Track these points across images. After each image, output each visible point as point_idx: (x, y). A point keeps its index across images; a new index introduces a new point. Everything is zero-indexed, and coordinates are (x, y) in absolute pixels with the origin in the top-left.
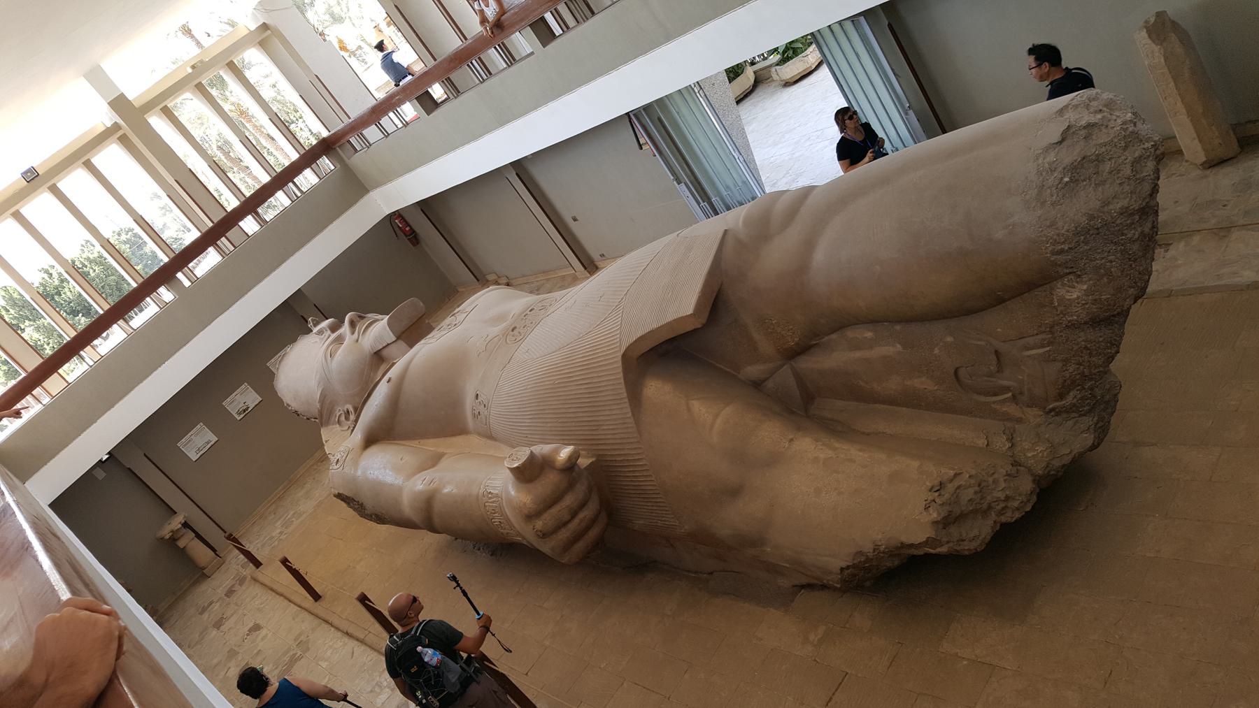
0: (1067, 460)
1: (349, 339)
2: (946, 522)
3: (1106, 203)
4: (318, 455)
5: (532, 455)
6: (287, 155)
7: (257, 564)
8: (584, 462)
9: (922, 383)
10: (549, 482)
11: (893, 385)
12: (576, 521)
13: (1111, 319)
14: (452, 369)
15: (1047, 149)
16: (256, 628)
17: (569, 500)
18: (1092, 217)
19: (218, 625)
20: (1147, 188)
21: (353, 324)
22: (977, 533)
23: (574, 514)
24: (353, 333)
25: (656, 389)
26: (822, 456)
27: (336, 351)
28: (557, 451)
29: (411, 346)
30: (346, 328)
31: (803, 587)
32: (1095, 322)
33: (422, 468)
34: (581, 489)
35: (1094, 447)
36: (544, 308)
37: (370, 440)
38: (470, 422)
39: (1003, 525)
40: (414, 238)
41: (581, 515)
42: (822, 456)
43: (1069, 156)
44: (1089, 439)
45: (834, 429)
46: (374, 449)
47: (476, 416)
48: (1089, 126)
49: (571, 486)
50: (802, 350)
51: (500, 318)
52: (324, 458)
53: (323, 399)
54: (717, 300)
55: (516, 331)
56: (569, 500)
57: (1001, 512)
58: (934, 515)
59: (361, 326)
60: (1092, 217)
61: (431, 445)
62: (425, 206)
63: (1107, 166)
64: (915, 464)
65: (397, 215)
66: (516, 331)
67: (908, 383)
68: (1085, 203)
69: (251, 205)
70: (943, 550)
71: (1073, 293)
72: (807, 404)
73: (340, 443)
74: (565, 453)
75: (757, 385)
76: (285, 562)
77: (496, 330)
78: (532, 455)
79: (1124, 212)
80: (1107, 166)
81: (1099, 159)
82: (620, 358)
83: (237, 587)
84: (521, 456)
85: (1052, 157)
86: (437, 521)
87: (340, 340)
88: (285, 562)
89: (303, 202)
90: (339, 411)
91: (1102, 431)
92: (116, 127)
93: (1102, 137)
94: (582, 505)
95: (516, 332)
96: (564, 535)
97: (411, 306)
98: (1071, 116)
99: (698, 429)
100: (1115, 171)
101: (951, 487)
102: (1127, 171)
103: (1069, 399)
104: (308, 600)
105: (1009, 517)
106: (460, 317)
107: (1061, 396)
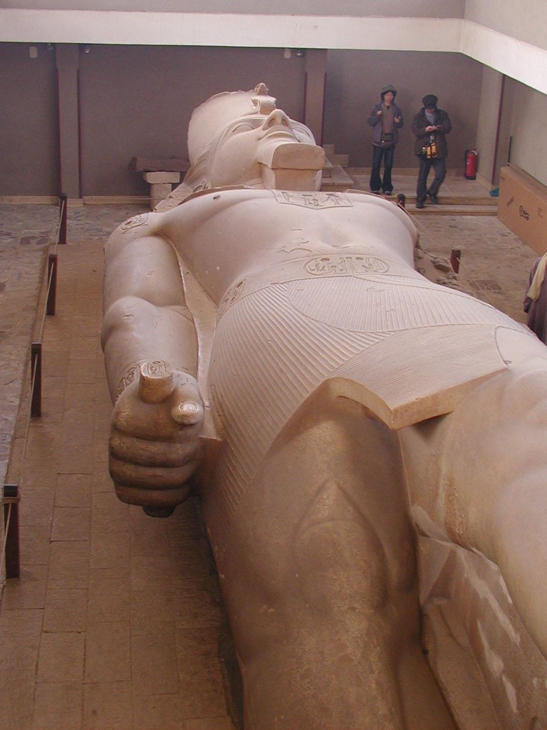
1: (259, 131)
5: (169, 380)
8: (210, 432)
9: (511, 691)
12: (150, 472)
14: (255, 240)
17: (156, 449)
21: (271, 122)
23: (152, 464)
24: (264, 129)
25: (325, 436)
26: (349, 650)
27: (243, 130)
28: (186, 399)
29: (278, 187)
34: (179, 451)
36: (367, 268)
41: (159, 471)
42: (349, 650)
46: (157, 242)
49: (169, 439)
53: (202, 160)
55: (330, 262)
56: (156, 449)
59: (278, 129)
61: (190, 285)
67: (504, 679)
77: (318, 245)
78: (169, 380)
82: (322, 380)
83: (33, 242)
86: (107, 347)
87: (255, 124)
95: (322, 264)
96: (130, 471)
99: (305, 510)
106: (330, 203)
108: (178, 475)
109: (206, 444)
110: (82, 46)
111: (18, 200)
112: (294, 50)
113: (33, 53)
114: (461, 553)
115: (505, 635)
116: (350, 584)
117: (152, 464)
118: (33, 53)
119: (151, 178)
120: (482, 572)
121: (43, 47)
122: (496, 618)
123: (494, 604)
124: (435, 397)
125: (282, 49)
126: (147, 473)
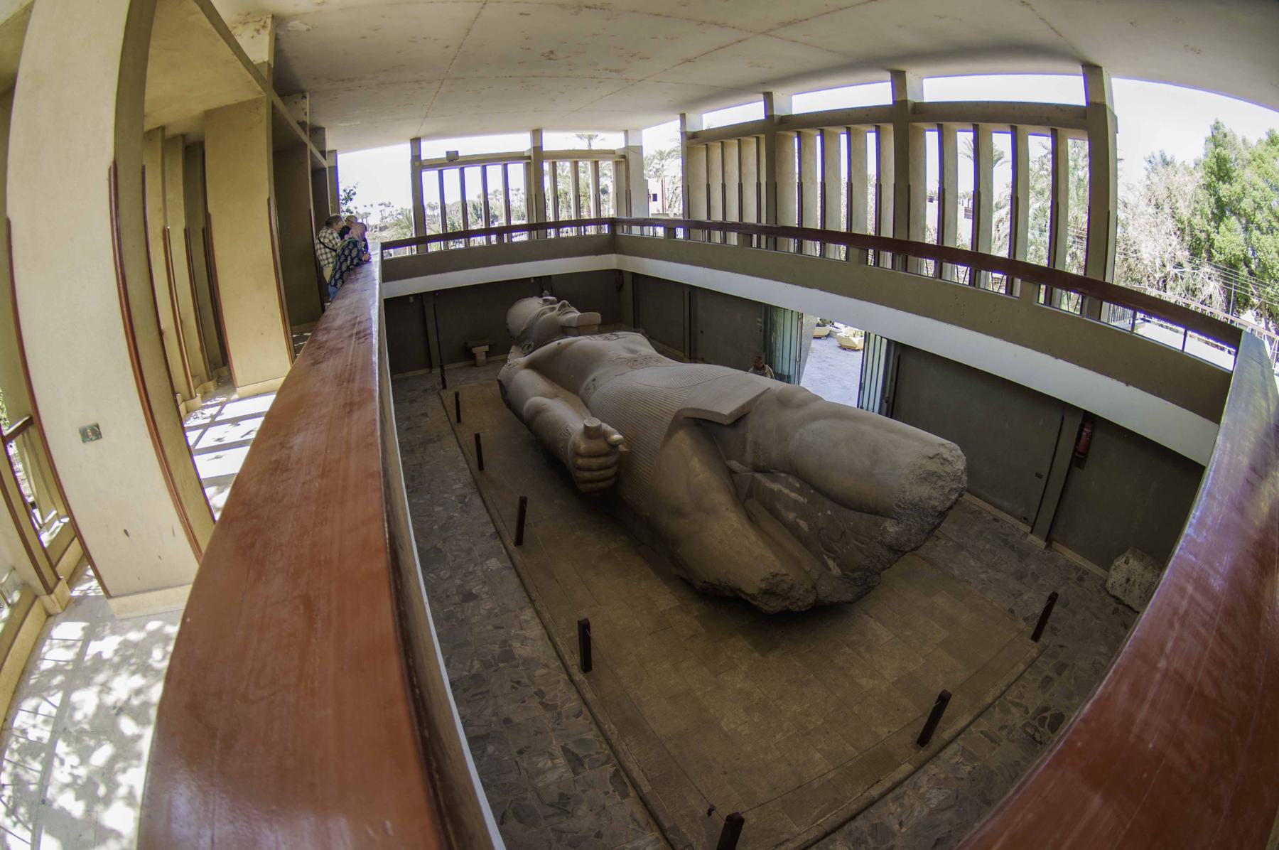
0: (835, 600)
2: (765, 592)
3: (930, 498)
4: (503, 357)
6: (589, 213)
7: (445, 387)
8: (622, 448)
9: (803, 524)
10: (599, 445)
11: (791, 516)
13: (897, 551)
15: (924, 457)
16: (426, 415)
17: (601, 460)
18: (921, 500)
19: (412, 401)
20: (948, 504)
22: (774, 606)
23: (600, 469)
30: (557, 306)
31: (682, 579)
32: (890, 548)
33: (544, 395)
34: (612, 459)
35: (850, 603)
37: (531, 365)
38: (582, 391)
39: (788, 610)
40: (620, 288)
43: (933, 466)
44: (849, 596)
45: (751, 519)
47: (587, 389)
48: (945, 459)
49: (607, 455)
50: (764, 471)
51: (633, 352)
52: (505, 361)
53: (523, 332)
54: (740, 418)
56: (601, 460)
57: (791, 604)
58: (763, 586)
60: (921, 500)
62: (636, 276)
63: (941, 483)
64: (773, 558)
65: (620, 271)
66: (635, 362)
68: (924, 491)
69: (558, 225)
70: (755, 603)
71: (891, 528)
72: (746, 497)
73: (517, 359)
74: (617, 436)
75: (731, 472)
76: (457, 395)
77: (629, 355)
79: (934, 507)
80: (941, 483)
81: (940, 477)
84: (594, 422)
85: (924, 461)
87: (553, 309)
88: (457, 395)
89: (580, 239)
90: (527, 342)
91: (859, 598)
92: (529, 158)
93: (948, 469)
94: (607, 467)
96: (587, 475)
97: (596, 317)
98: (942, 450)
99: (688, 473)
100: (943, 487)
101: (779, 578)
102: (947, 490)
103: (856, 575)
104: (454, 419)
105: (794, 608)
107: (853, 571)
108: (610, 472)
109: (622, 454)
110: (435, 292)
111: (410, 374)
112: (535, 278)
113: (411, 299)
114: (758, 476)
115: (796, 502)
116: (720, 498)
117: (600, 469)
118: (411, 299)
119: (474, 350)
120: (775, 480)
121: (416, 296)
122: (787, 496)
123: (786, 491)
124: (743, 407)
125: (529, 279)
126: (596, 474)
